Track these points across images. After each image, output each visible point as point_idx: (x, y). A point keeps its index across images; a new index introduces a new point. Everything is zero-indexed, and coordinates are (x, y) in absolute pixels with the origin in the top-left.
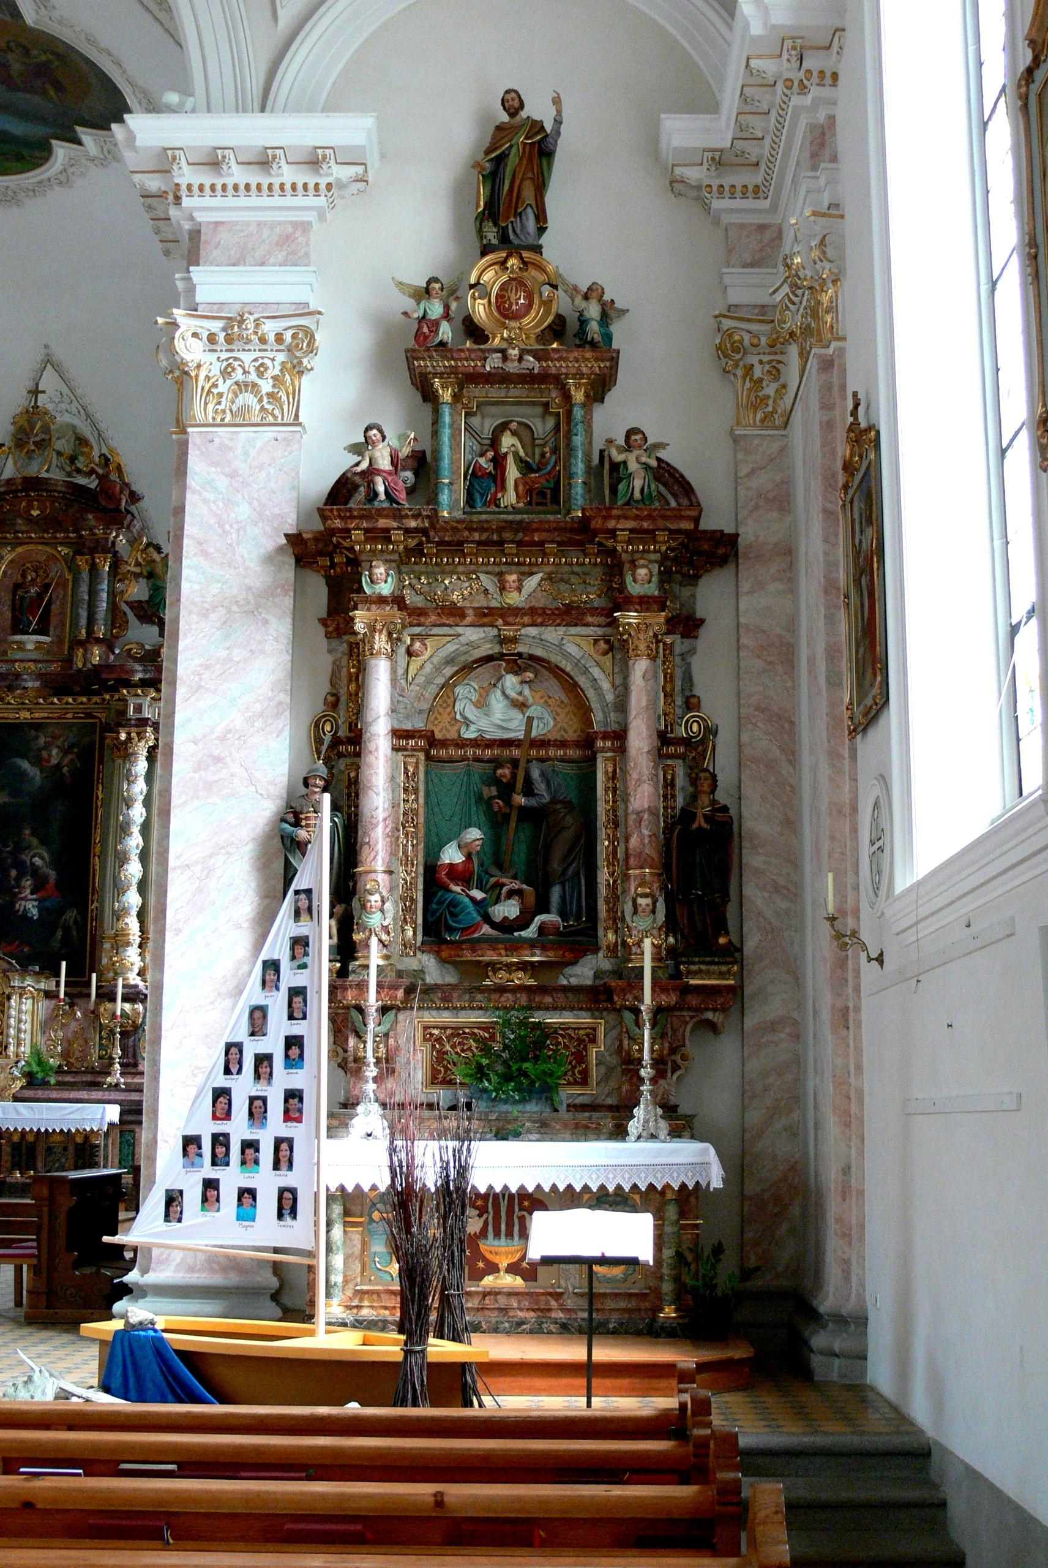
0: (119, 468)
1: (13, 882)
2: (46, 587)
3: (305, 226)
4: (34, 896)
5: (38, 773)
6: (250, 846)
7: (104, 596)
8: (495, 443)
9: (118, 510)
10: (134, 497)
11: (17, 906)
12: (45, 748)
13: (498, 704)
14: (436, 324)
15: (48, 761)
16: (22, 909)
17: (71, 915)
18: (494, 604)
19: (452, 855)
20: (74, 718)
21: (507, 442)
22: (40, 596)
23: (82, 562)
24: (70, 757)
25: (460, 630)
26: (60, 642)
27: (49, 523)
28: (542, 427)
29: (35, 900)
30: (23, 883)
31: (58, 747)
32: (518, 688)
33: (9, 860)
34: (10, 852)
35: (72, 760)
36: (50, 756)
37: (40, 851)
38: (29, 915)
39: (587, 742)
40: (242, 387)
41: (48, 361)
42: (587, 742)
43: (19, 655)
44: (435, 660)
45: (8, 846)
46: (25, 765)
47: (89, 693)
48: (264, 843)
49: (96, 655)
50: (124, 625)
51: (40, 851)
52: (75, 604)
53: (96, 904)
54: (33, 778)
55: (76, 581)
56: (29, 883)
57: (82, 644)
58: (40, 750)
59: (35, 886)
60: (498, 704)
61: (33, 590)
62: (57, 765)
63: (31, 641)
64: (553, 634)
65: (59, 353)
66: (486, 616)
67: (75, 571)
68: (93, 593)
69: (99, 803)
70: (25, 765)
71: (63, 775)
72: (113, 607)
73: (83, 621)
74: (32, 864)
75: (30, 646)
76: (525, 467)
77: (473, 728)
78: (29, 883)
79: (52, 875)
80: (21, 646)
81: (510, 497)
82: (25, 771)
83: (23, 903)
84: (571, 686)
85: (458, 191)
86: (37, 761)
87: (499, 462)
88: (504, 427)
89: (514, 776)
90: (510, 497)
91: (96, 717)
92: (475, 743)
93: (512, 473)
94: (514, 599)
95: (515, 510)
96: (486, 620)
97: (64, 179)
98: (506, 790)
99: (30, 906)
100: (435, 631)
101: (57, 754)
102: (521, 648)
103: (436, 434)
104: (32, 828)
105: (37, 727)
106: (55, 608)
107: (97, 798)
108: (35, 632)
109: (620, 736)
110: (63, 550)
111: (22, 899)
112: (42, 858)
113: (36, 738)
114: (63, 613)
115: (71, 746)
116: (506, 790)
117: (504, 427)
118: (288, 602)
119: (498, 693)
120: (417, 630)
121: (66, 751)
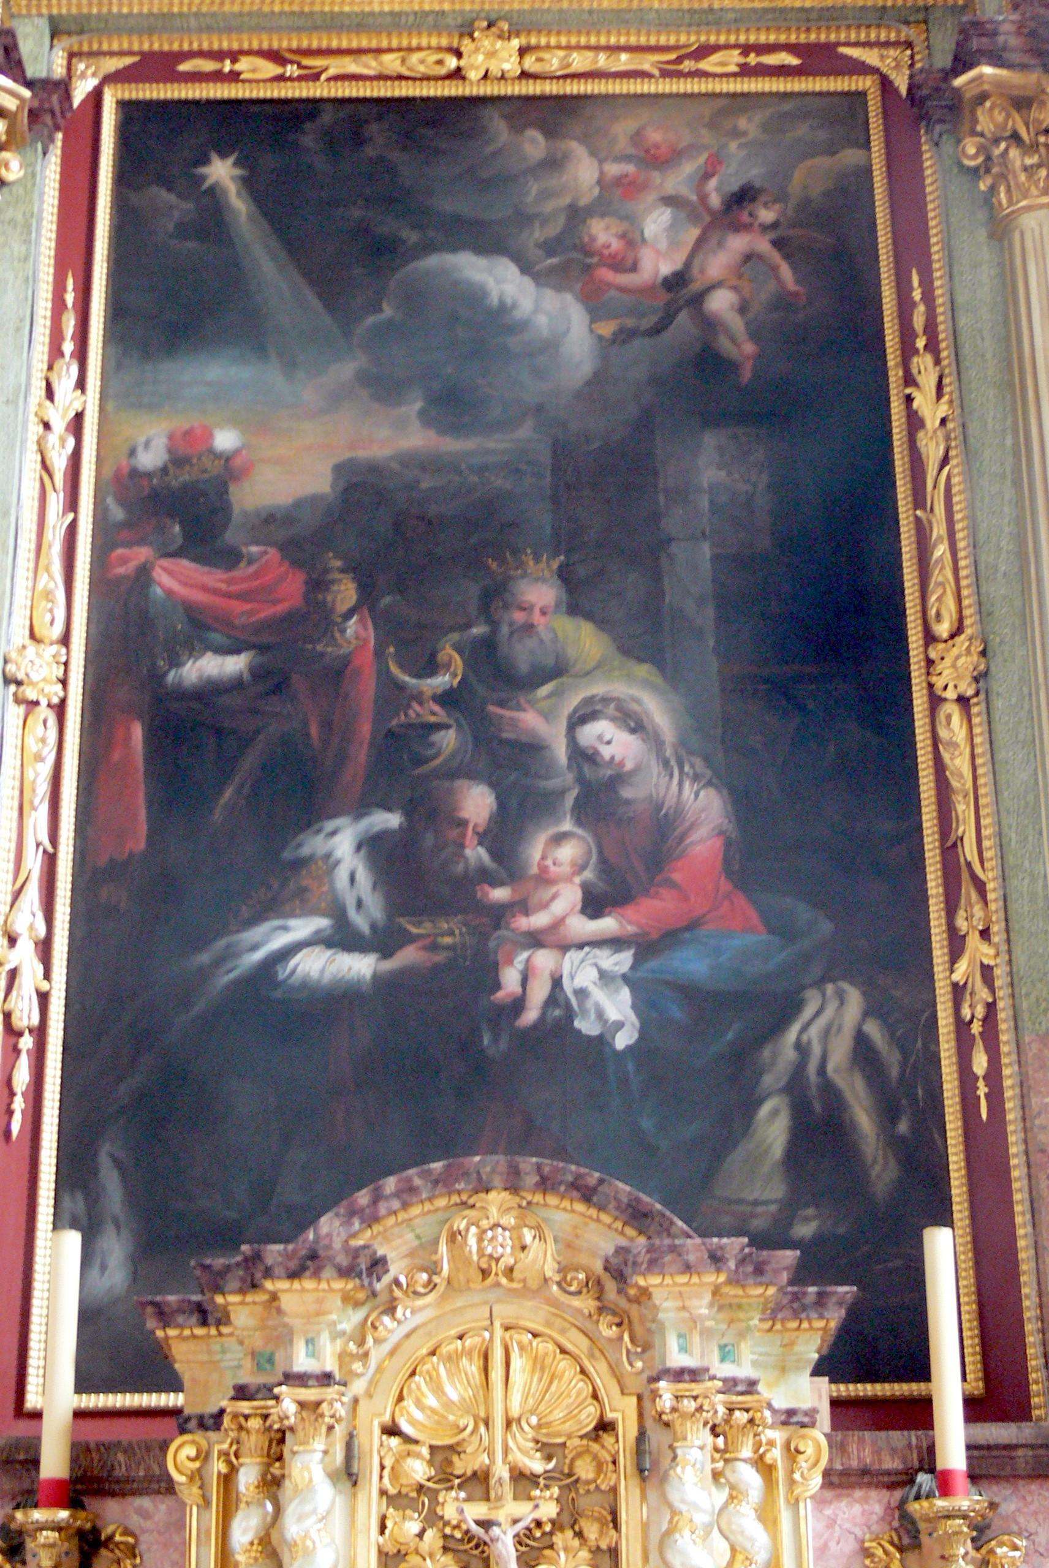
1: (476, 854)
4: (608, 924)
5: (576, 316)
11: (510, 979)
12: (600, 207)
15: (625, 264)
16: (539, 993)
20: (745, 71)
24: (738, 243)
29: (615, 943)
30: (535, 850)
31: (670, 201)
33: (448, 740)
34: (447, 699)
35: (748, 257)
36: (632, 240)
37: (619, 689)
38: (587, 1026)
45: (431, 667)
51: (619, 689)
53: (978, 951)
54: (551, 346)
56: (567, 853)
58: (577, 215)
59: (605, 866)
62: (677, 281)
69: (932, 449)
71: (709, 325)
74: (583, 756)
78: (567, 853)
82: (503, 309)
83: (544, 960)
91: (861, 68)
99: (586, 977)
101: (673, 227)
104: (565, 575)
107: (915, 422)
111: (536, 940)
112: (635, 724)
113: (553, 163)
115: (743, 197)
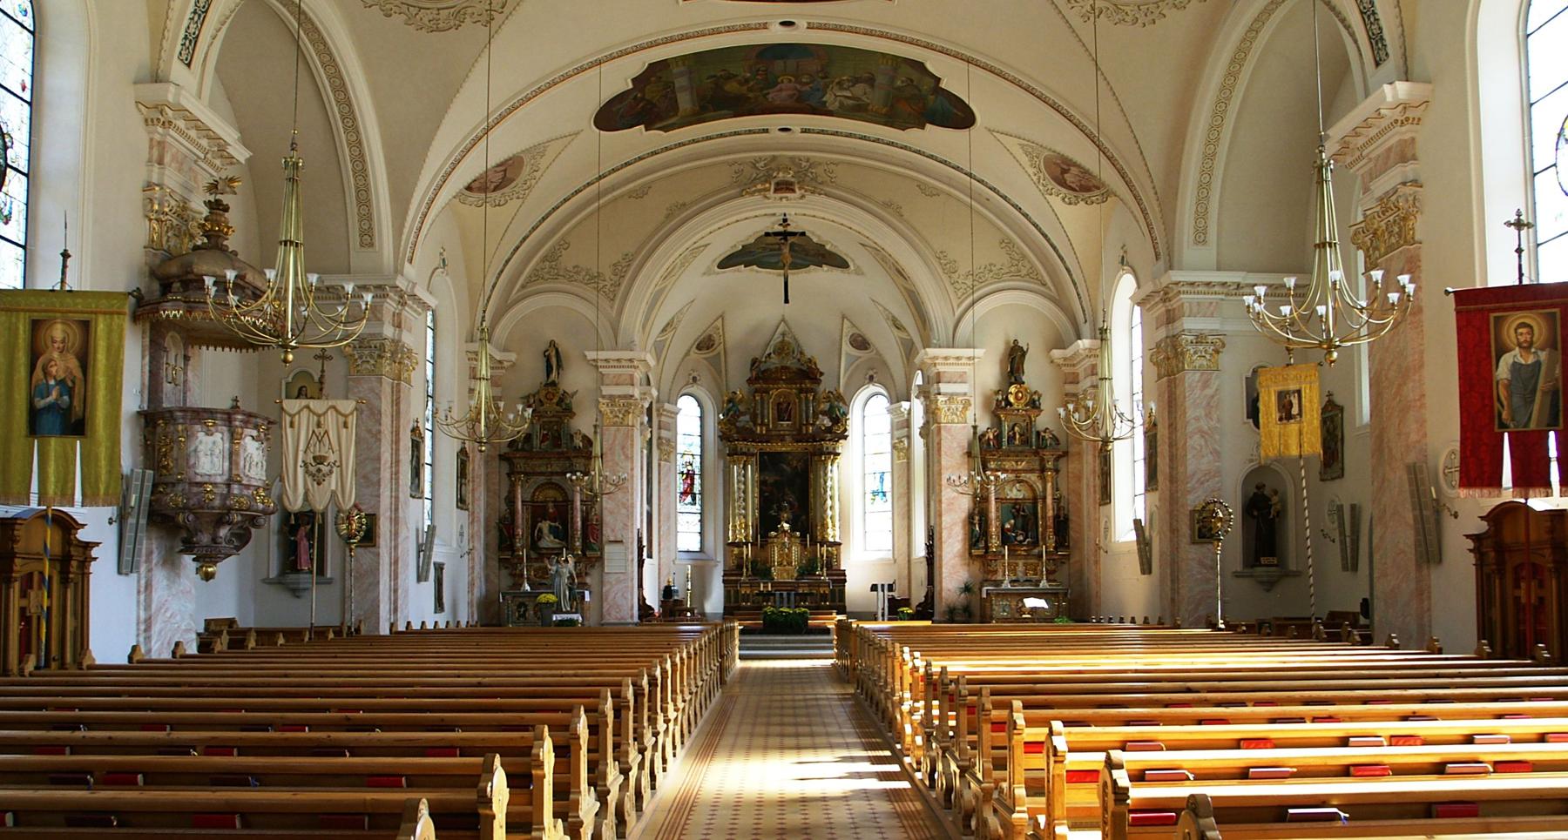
0: (815, 364)
2: (789, 404)
3: (965, 373)
6: (961, 524)
8: (1013, 429)
9: (816, 379)
10: (822, 374)
13: (1015, 490)
17: (804, 517)
19: (1008, 526)
21: (1016, 428)
22: (787, 408)
23: (803, 396)
26: (794, 423)
27: (789, 381)
28: (1024, 424)
39: (1035, 500)
40: (953, 414)
41: (783, 320)
42: (1035, 500)
46: (785, 466)
47: (807, 442)
50: (817, 418)
52: (801, 411)
55: (800, 402)
60: (1015, 490)
61: (785, 405)
63: (785, 423)
64: (1028, 475)
65: (787, 318)
66: (1013, 471)
67: (800, 399)
68: (807, 408)
70: (785, 466)
76: (1021, 435)
79: (796, 504)
81: (1017, 442)
84: (1031, 486)
85: (1001, 362)
86: (789, 465)
87: (1015, 434)
88: (1015, 425)
90: (1017, 442)
93: (1018, 436)
94: (1020, 467)
97: (809, 271)
98: (1018, 511)
105: (788, 453)
109: (1044, 498)
116: (1018, 511)
117: (1015, 425)
118: (966, 466)
121: (800, 461)
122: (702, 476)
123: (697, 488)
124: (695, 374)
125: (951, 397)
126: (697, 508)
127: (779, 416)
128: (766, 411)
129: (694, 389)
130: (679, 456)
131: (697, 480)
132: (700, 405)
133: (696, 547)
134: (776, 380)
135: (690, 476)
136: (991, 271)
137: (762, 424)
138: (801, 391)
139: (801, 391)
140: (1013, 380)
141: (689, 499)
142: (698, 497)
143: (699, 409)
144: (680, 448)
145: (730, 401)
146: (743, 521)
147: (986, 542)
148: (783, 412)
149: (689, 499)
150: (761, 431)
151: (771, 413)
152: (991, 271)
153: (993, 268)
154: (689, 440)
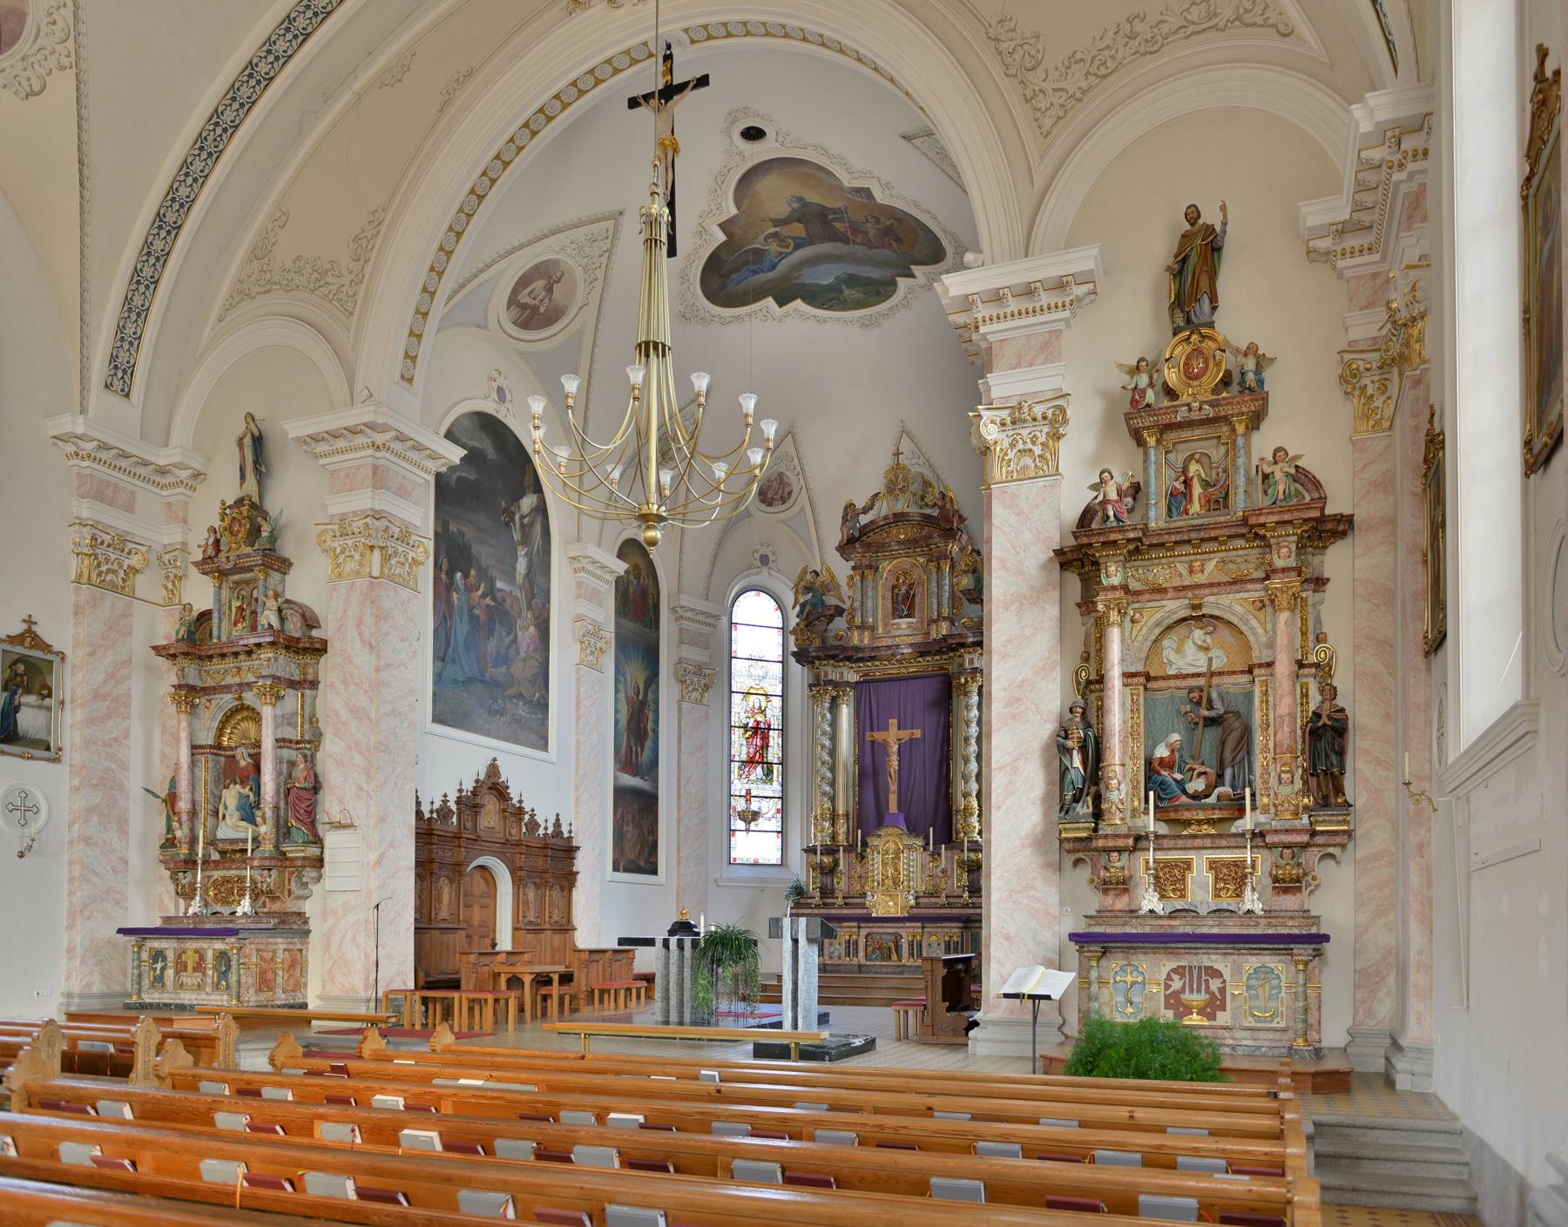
2: (912, 585)
7: (947, 588)
14: (1144, 391)
18: (1187, 583)
22: (907, 592)
23: (932, 566)
25: (1164, 603)
26: (922, 622)
27: (912, 543)
32: (1203, 638)
43: (897, 633)
44: (1149, 624)
48: (1046, 749)
49: (944, 628)
57: (935, 621)
61: (904, 589)
63: (904, 622)
68: (940, 587)
72: (953, 595)
73: (935, 607)
75: (904, 626)
77: (1174, 667)
80: (898, 626)
89: (1201, 697)
92: (1176, 677)
95: (1199, 516)
96: (1181, 594)
100: (1149, 605)
102: (1205, 611)
103: (1146, 469)
106: (917, 599)
108: (907, 616)
110: (922, 560)
114: (922, 602)
119: (1190, 642)
120: (1137, 605)
122: (783, 732)
123: (774, 754)
124: (763, 550)
125: (1016, 418)
126: (775, 788)
127: (895, 609)
128: (870, 603)
129: (763, 577)
130: (736, 698)
131: (775, 739)
132: (781, 607)
133: (774, 856)
134: (881, 547)
135: (759, 732)
136: (1132, 36)
137: (863, 627)
138: (930, 560)
139: (930, 560)
140: (1180, 321)
141: (759, 771)
142: (777, 769)
143: (779, 613)
144: (742, 675)
145: (808, 589)
146: (828, 805)
147: (1098, 799)
148: (904, 603)
149: (759, 771)
150: (862, 641)
151: (878, 603)
152: (1132, 36)
153: (1139, 27)
154: (758, 669)
